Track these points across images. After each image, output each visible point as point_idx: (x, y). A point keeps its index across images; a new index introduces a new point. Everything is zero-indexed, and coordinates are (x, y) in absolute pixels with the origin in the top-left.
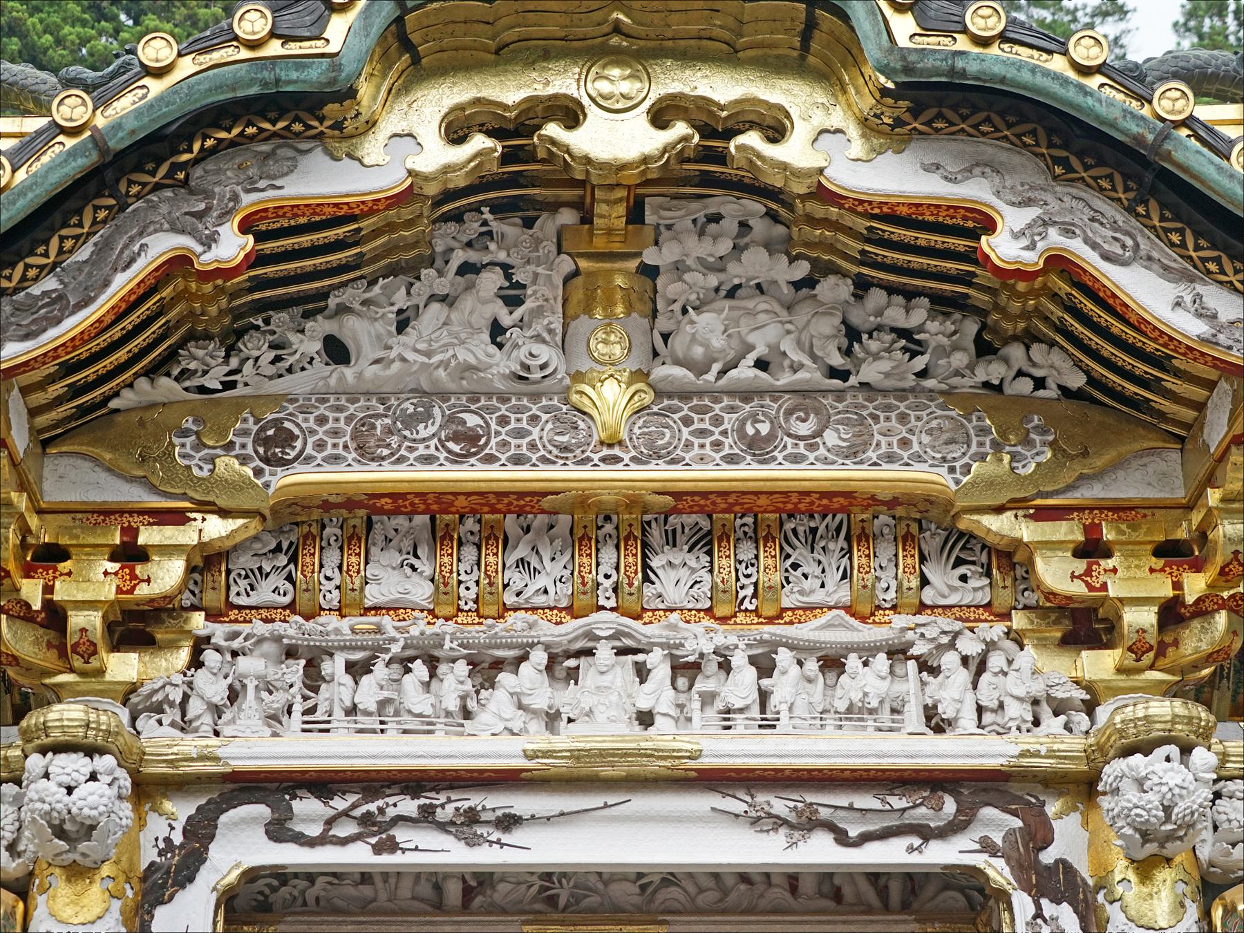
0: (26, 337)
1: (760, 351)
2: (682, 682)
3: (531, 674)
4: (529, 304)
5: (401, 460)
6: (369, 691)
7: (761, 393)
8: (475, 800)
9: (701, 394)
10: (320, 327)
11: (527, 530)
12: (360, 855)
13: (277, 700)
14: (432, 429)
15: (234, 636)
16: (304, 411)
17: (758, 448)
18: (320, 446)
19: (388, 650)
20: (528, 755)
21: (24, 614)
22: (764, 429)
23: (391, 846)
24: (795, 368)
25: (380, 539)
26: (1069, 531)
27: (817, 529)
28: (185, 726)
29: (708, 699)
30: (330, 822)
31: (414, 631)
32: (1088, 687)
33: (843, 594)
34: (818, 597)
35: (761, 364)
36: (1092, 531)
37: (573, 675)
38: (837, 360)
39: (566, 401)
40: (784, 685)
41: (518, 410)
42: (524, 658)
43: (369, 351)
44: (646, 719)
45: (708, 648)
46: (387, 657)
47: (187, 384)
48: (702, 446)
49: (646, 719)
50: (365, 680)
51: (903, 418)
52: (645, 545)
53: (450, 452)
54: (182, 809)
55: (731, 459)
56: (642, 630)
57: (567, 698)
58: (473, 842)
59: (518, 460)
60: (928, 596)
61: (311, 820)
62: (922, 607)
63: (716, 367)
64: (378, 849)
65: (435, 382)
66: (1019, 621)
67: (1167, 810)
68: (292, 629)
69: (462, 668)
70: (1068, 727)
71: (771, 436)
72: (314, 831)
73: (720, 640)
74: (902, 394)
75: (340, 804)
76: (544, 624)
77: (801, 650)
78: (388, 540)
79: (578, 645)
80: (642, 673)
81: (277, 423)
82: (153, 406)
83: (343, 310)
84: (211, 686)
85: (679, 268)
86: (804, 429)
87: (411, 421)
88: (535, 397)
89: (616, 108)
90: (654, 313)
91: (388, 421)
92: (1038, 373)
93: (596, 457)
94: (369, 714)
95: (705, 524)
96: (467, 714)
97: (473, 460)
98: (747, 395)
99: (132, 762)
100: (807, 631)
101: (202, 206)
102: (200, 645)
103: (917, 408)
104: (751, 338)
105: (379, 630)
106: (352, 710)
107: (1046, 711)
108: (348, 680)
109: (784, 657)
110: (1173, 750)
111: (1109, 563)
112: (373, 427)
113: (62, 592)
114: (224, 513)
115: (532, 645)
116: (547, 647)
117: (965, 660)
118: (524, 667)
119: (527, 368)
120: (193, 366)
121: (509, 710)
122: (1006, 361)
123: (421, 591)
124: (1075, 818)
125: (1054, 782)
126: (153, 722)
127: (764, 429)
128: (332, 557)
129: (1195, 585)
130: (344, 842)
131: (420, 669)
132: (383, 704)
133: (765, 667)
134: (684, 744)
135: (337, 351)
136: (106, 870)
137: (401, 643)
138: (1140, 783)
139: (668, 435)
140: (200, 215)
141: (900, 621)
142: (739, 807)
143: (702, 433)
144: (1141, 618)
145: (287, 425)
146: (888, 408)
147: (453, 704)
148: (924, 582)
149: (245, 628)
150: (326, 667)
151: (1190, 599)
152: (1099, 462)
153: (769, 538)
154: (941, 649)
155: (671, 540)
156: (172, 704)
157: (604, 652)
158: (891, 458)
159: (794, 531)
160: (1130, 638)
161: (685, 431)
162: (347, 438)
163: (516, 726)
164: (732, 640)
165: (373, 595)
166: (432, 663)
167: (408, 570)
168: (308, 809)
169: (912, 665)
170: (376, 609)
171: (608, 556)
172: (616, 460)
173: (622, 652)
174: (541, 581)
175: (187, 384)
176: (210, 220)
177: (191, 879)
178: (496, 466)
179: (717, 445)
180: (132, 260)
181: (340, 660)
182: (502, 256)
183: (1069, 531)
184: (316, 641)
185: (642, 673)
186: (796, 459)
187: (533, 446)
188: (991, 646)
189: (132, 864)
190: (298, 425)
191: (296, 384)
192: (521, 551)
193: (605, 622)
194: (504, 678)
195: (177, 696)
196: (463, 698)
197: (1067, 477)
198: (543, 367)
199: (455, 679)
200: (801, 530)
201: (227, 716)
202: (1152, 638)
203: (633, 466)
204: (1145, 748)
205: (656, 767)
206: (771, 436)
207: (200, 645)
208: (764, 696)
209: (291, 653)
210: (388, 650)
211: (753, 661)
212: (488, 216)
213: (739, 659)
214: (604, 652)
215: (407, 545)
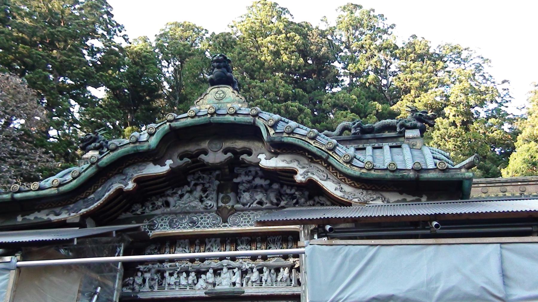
0: (86, 208)
3: (210, 274)
5: (179, 228)
10: (164, 199)
11: (210, 242)
14: (186, 221)
16: (159, 217)
19: (177, 271)
25: (178, 246)
27: (274, 239)
40: (265, 276)
42: (208, 271)
44: (234, 284)
45: (247, 267)
46: (177, 272)
47: (134, 213)
48: (245, 222)
53: (189, 225)
55: (251, 225)
57: (218, 280)
63: (249, 204)
65: (187, 210)
73: (250, 265)
76: (213, 263)
77: (269, 268)
78: (180, 245)
79: (220, 267)
91: (176, 219)
92: (322, 202)
93: (221, 225)
94: (173, 285)
95: (250, 239)
97: (194, 227)
101: (124, 177)
106: (169, 284)
109: (265, 269)
112: (173, 221)
115: (209, 268)
118: (208, 274)
119: (206, 206)
120: (134, 209)
126: (125, 289)
132: (175, 283)
133: (261, 271)
137: (180, 268)
139: (237, 220)
140: (124, 180)
143: (245, 219)
145: (155, 221)
147: (190, 282)
149: (148, 266)
156: (130, 284)
157: (225, 270)
159: (270, 240)
161: (241, 219)
162: (168, 223)
164: (253, 265)
166: (188, 273)
167: (184, 252)
173: (229, 269)
175: (134, 213)
176: (126, 181)
178: (200, 228)
180: (110, 190)
182: (202, 182)
184: (162, 269)
190: (157, 221)
191: (158, 212)
194: (203, 276)
195: (131, 282)
198: (211, 205)
200: (271, 240)
203: (230, 227)
210: (177, 271)
211: (258, 270)
212: (200, 173)
213: (254, 270)
215: (183, 246)
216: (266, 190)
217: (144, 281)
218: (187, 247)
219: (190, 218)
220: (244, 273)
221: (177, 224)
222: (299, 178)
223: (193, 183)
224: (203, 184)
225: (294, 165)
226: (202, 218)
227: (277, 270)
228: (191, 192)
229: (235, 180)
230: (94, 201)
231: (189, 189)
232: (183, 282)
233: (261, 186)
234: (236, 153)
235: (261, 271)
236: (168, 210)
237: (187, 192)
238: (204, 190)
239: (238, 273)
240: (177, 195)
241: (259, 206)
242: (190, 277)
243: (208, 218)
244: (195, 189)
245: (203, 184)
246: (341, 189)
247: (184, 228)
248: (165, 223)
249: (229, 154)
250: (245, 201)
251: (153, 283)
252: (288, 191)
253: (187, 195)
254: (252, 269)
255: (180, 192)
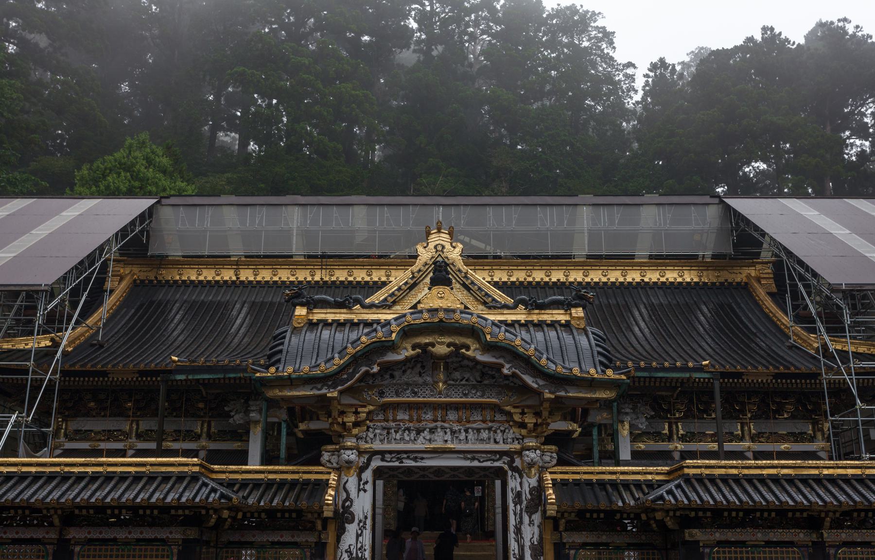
1: (466, 378)
2: (453, 434)
4: (426, 369)
6: (398, 436)
7: (466, 385)
8: (416, 455)
9: (456, 385)
10: (390, 372)
12: (397, 464)
13: (382, 437)
15: (374, 425)
16: (387, 387)
17: (466, 395)
18: (389, 394)
20: (426, 448)
21: (338, 423)
22: (467, 392)
23: (402, 462)
24: (473, 381)
26: (519, 410)
28: (366, 442)
29: (457, 437)
30: (392, 458)
31: (406, 426)
32: (523, 436)
33: (481, 419)
34: (476, 419)
35: (467, 380)
36: (523, 410)
37: (434, 432)
38: (479, 380)
39: (432, 386)
41: (424, 388)
42: (425, 429)
43: (397, 378)
44: (446, 441)
49: (446, 441)
50: (398, 434)
51: (491, 390)
52: (447, 409)
54: (366, 456)
55: (461, 397)
56: (446, 425)
58: (416, 462)
59: (424, 397)
60: (495, 419)
61: (388, 458)
62: (493, 421)
64: (400, 463)
66: (511, 423)
67: (532, 461)
68: (384, 424)
69: (414, 432)
70: (519, 443)
71: (468, 393)
72: (389, 460)
73: (459, 428)
74: (491, 385)
75: (393, 455)
80: (446, 433)
81: (382, 390)
82: (360, 386)
83: (394, 370)
84: (371, 435)
85: (453, 362)
86: (474, 392)
87: (406, 390)
88: (427, 385)
89: (442, 343)
90: (448, 369)
95: (457, 406)
96: (415, 440)
98: (464, 385)
99: (357, 448)
100: (474, 425)
102: (368, 427)
103: (494, 388)
104: (465, 376)
105: (399, 425)
107: (515, 440)
108: (394, 434)
109: (470, 430)
110: (534, 451)
111: (526, 415)
113: (346, 420)
114: (372, 406)
116: (429, 428)
117: (501, 431)
118: (425, 432)
121: (423, 440)
122: (509, 380)
123: (407, 417)
124: (519, 458)
125: (516, 452)
127: (467, 392)
128: (391, 411)
129: (540, 421)
130: (394, 462)
131: (407, 432)
132: (400, 438)
134: (452, 446)
135: (392, 376)
136: (354, 467)
138: (528, 456)
141: (490, 424)
142: (462, 456)
144: (530, 426)
146: (488, 388)
147: (413, 438)
148: (495, 416)
150: (391, 431)
151: (538, 423)
152: (525, 398)
153: (468, 409)
154: (497, 429)
155: (451, 409)
157: (439, 430)
158: (488, 397)
160: (529, 429)
163: (424, 442)
165: (398, 418)
168: (388, 456)
169: (492, 432)
170: (400, 421)
171: (440, 412)
172: (441, 397)
174: (428, 416)
177: (368, 468)
179: (459, 395)
181: (393, 431)
183: (519, 410)
184: (389, 427)
185: (446, 433)
186: (472, 397)
187: (426, 395)
188: (506, 429)
189: (358, 466)
191: (385, 382)
192: (425, 410)
193: (439, 424)
194: (422, 434)
195: (364, 436)
196: (415, 437)
197: (518, 401)
199: (414, 433)
201: (374, 440)
202: (532, 429)
204: (529, 450)
205: (448, 450)
206: (468, 393)
207: (368, 427)
208: (467, 437)
209: (384, 428)
211: (465, 430)
213: (462, 431)
214: (439, 430)
216: (471, 369)
217: (375, 436)
218: (407, 410)
219: (412, 390)
220: (453, 432)
221: (402, 393)
222: (505, 371)
223: (413, 360)
224: (422, 362)
225: (501, 361)
226: (421, 390)
227: (478, 430)
228: (412, 368)
229: (447, 360)
230: (348, 380)
231: (411, 366)
232: (407, 438)
233: (468, 366)
234: (458, 347)
235: (466, 431)
236: (394, 381)
237: (409, 368)
238: (423, 367)
239: (449, 433)
240: (402, 370)
241: (467, 383)
242: (412, 435)
243: (427, 390)
244: (415, 365)
245: (422, 362)
246: (537, 383)
247: (408, 397)
248: (392, 392)
249: (452, 348)
250: (456, 378)
251: (382, 437)
252: (490, 372)
253: (409, 371)
254: (460, 430)
255: (403, 368)
